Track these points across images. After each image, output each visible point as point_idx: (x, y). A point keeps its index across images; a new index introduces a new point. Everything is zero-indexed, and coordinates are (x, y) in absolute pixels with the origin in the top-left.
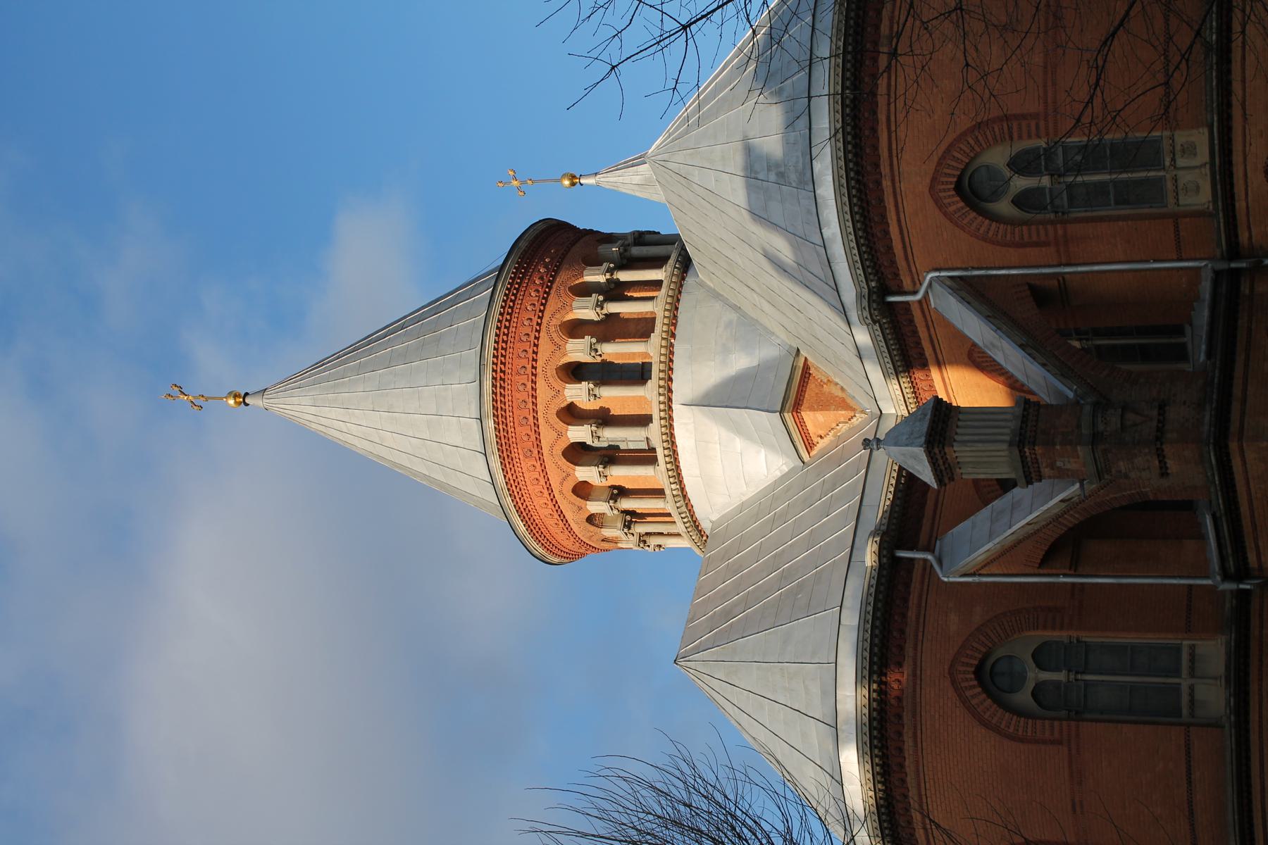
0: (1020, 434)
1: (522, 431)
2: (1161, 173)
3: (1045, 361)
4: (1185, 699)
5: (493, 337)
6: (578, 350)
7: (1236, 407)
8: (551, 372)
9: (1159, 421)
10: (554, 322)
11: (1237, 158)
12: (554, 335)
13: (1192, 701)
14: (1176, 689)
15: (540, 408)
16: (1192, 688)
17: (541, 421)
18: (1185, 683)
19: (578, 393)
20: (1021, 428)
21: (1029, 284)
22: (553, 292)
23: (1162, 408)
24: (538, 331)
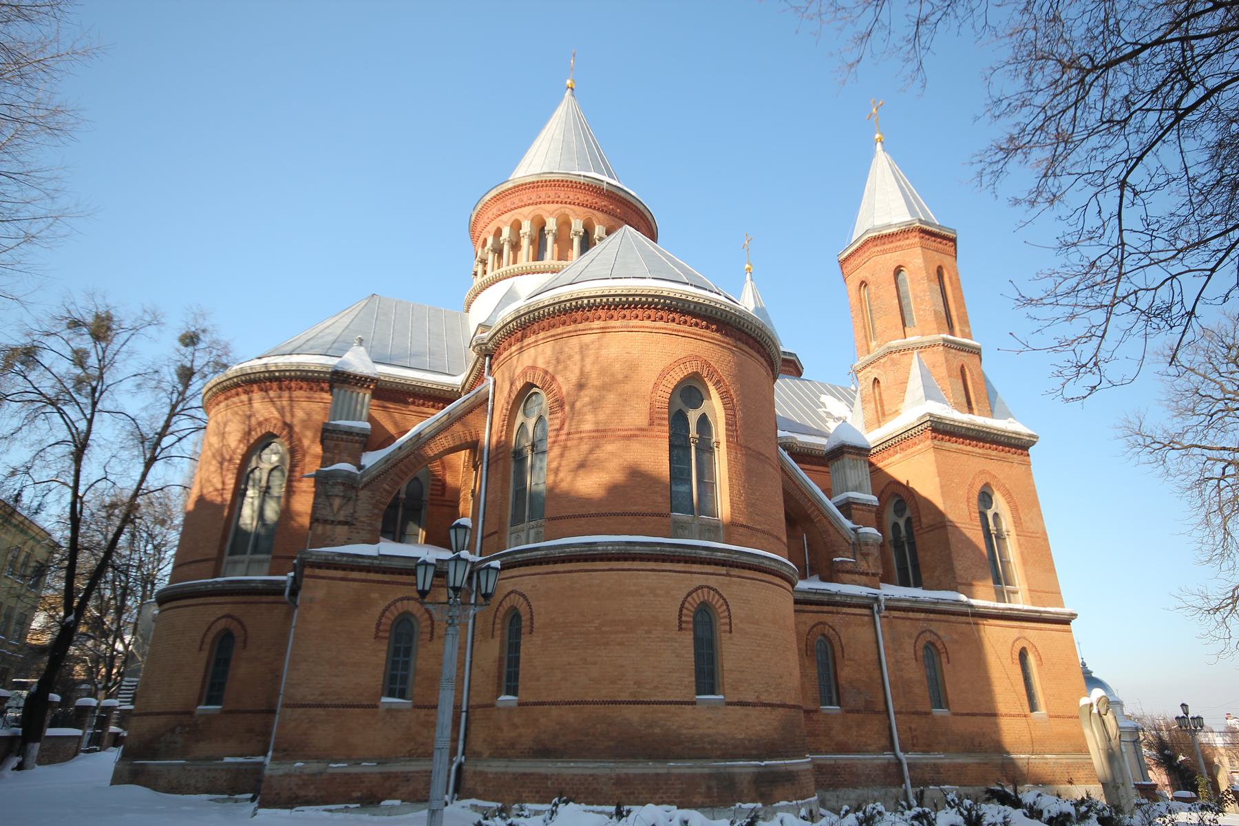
0: (334, 431)
1: (508, 204)
2: (526, 520)
3: (402, 449)
4: (236, 557)
5: (556, 179)
6: (551, 225)
7: (340, 574)
8: (538, 212)
9: (333, 522)
10: (567, 210)
11: (523, 570)
12: (559, 211)
13: (235, 562)
14: (245, 553)
15: (519, 210)
16: (243, 562)
17: (513, 212)
18: (246, 557)
19: (526, 227)
20: (340, 431)
21: (479, 440)
22: (587, 209)
23: (346, 523)
24: (561, 203)
